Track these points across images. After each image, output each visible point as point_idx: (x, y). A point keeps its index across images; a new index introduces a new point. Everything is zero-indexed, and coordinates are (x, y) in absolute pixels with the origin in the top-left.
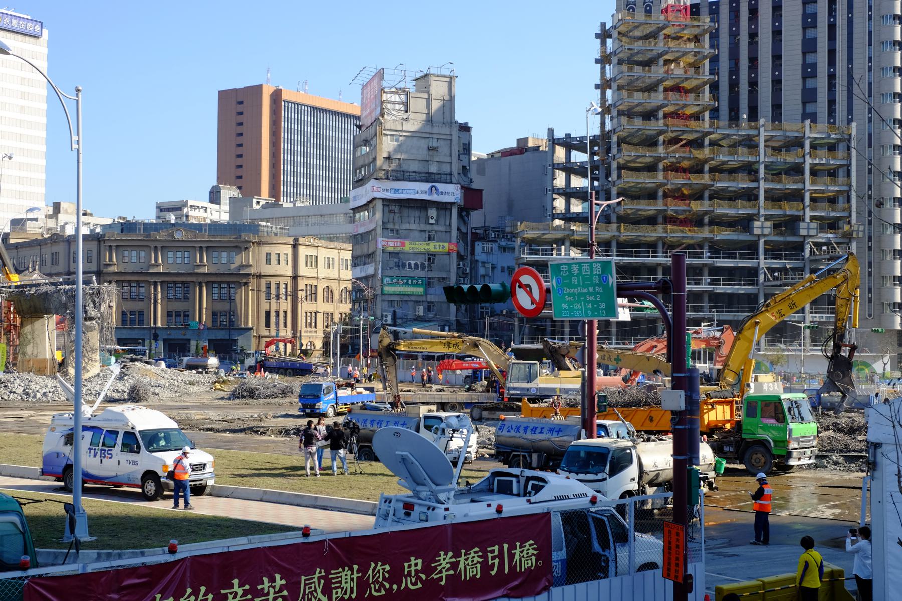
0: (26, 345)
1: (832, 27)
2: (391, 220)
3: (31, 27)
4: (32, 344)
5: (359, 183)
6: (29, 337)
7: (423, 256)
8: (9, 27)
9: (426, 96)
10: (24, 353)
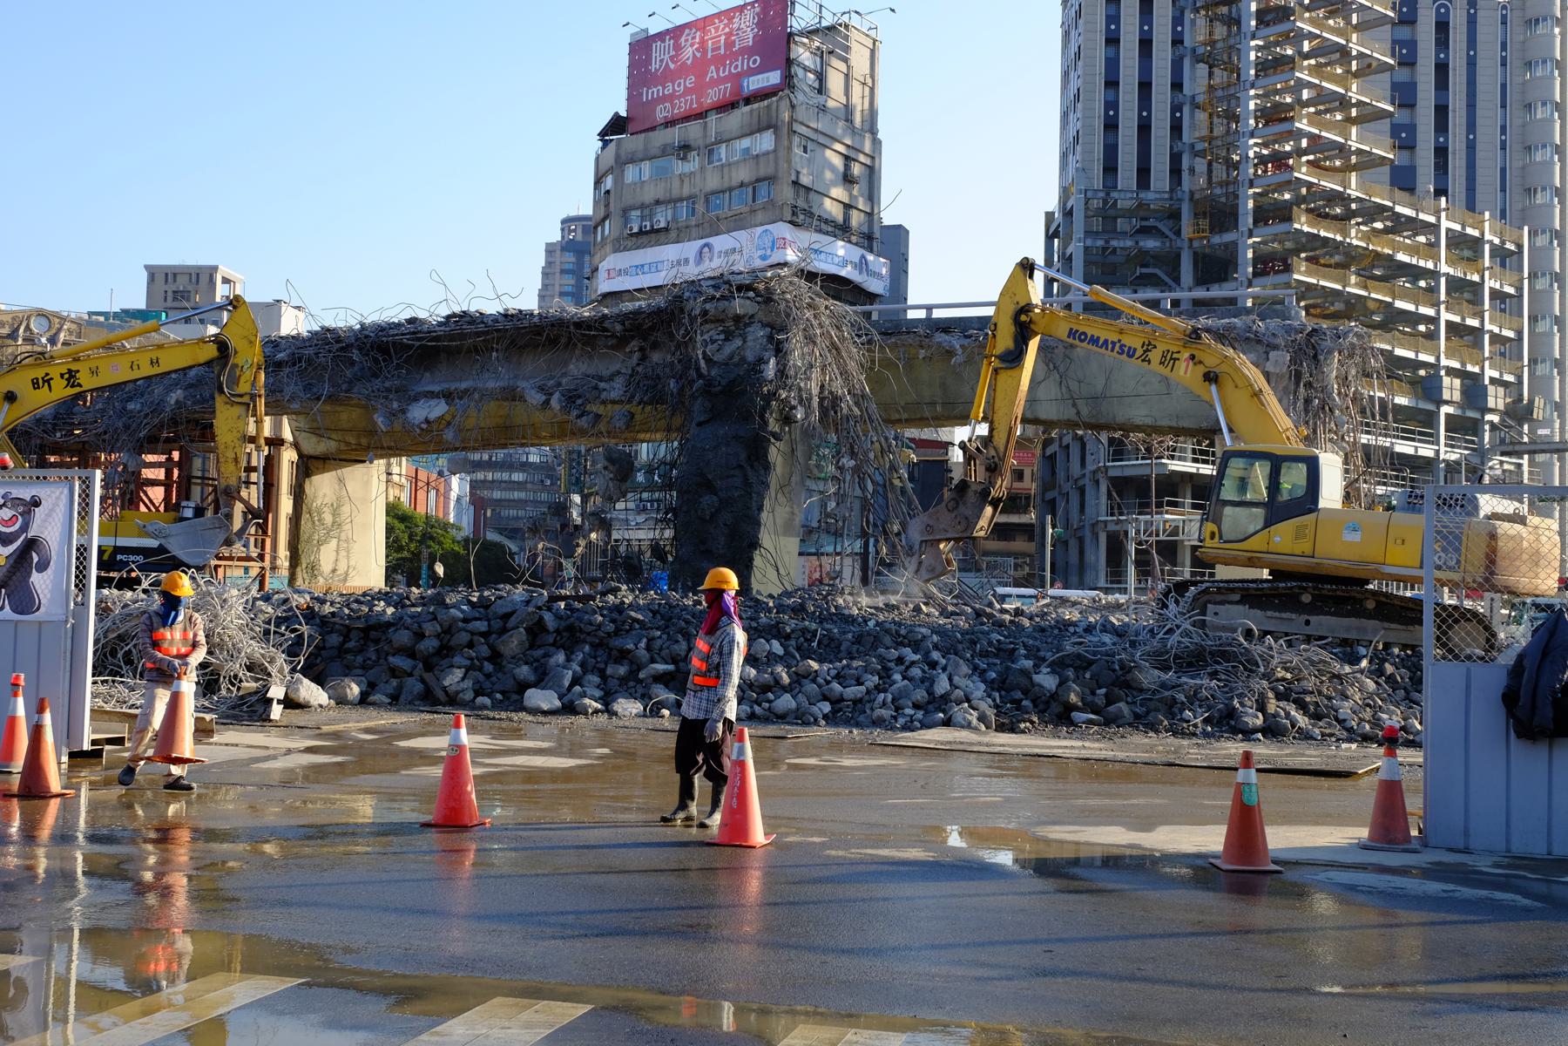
0: (320, 543)
1: (1442, 69)
4: (334, 543)
6: (328, 518)
9: (843, 67)
10: (313, 569)
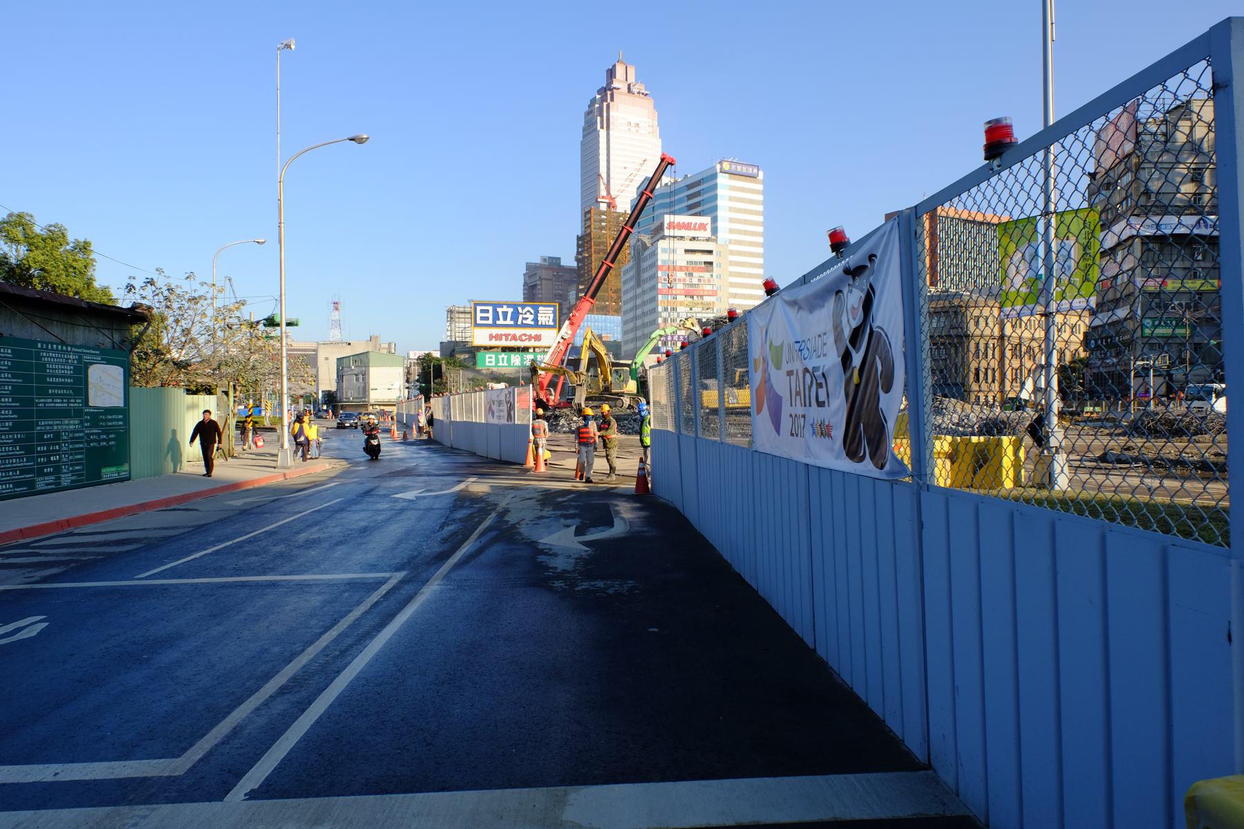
2: (1150, 259)
3: (750, 171)
5: (1106, 226)
7: (1188, 295)
8: (735, 172)
